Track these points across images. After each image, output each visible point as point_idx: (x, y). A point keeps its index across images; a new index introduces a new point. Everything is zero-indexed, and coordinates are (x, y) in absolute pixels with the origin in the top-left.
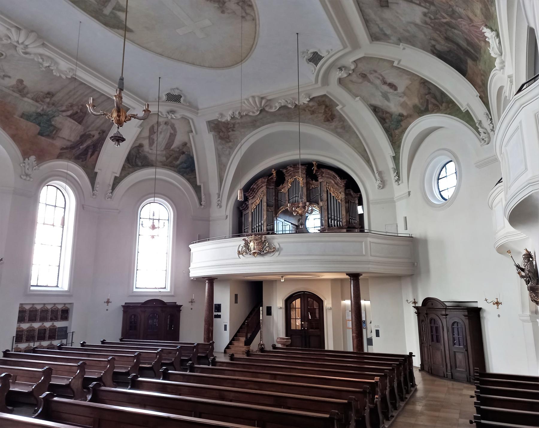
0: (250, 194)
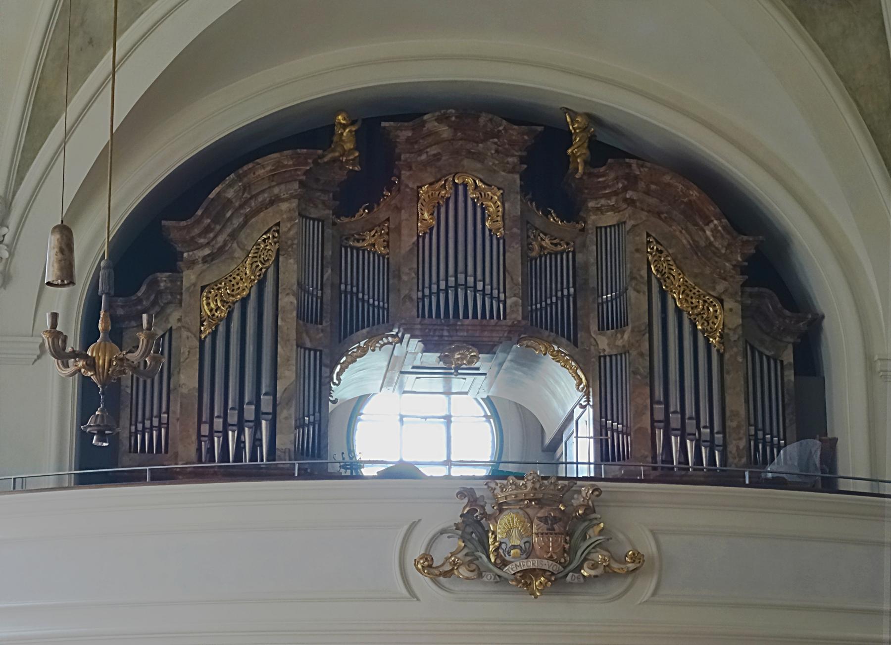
0: (196, 231)
